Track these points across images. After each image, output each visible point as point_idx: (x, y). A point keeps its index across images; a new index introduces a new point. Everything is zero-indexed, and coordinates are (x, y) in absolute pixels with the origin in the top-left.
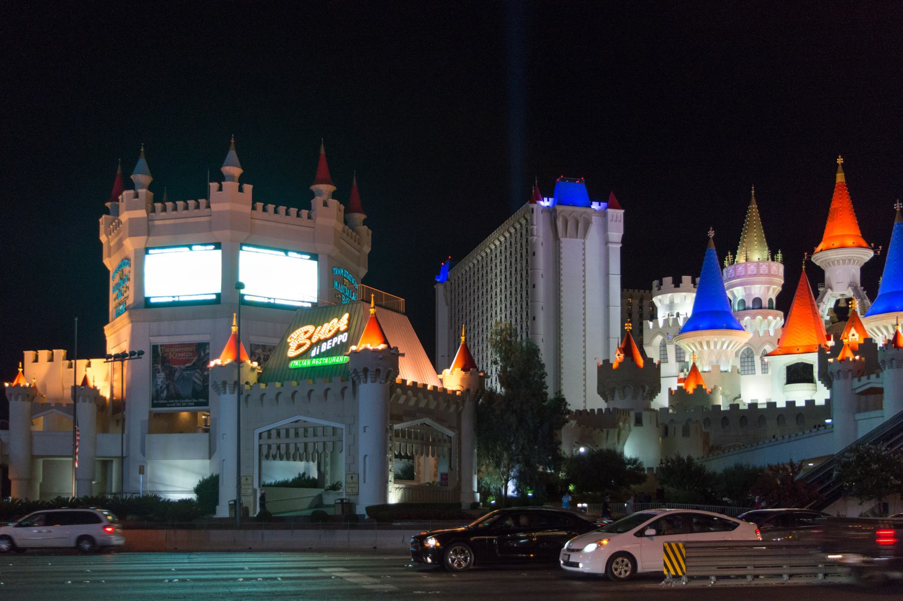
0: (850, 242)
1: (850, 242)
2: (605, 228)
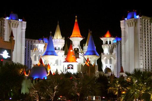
0: (78, 36)
1: (78, 36)
2: (22, 26)
